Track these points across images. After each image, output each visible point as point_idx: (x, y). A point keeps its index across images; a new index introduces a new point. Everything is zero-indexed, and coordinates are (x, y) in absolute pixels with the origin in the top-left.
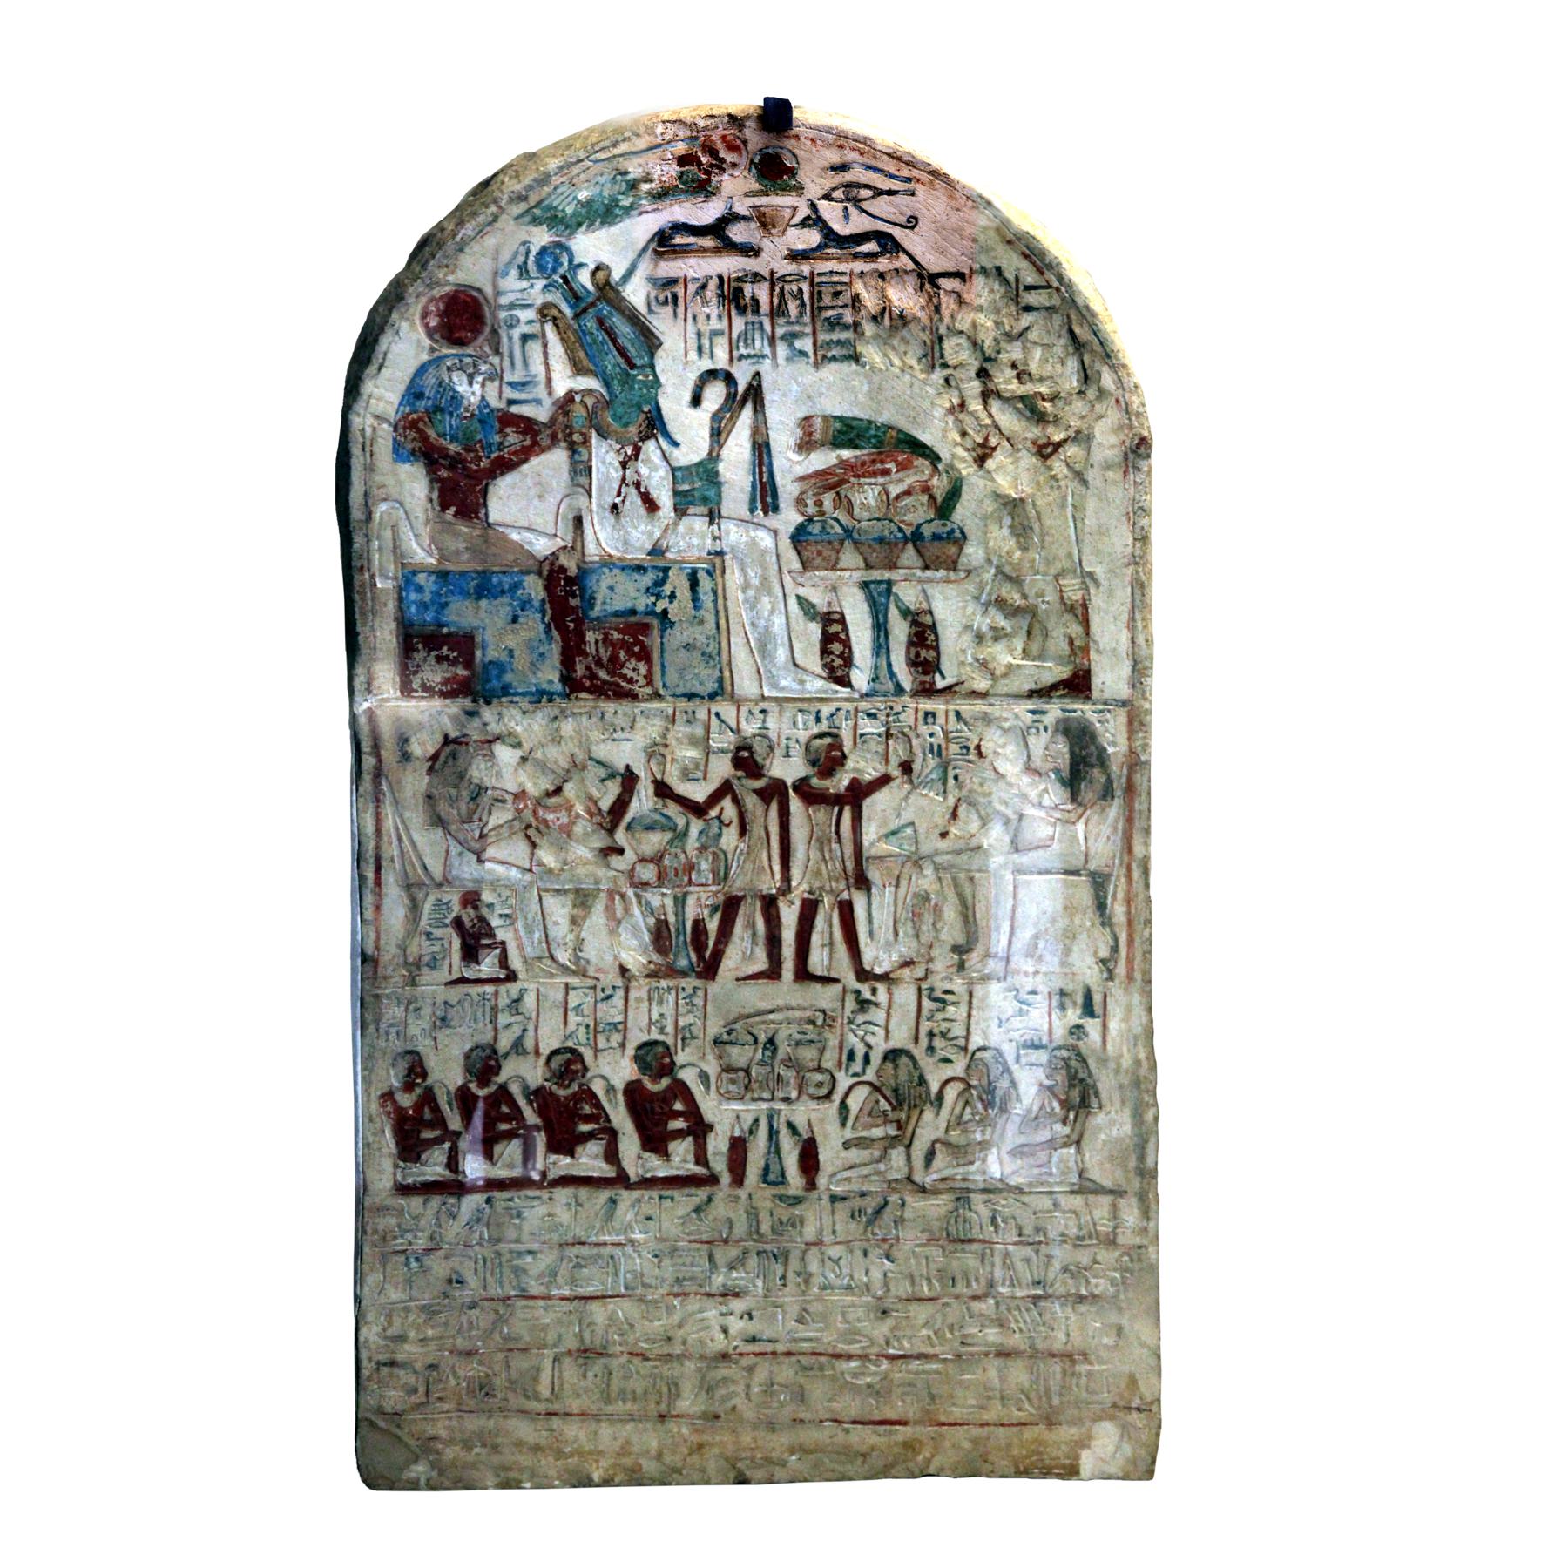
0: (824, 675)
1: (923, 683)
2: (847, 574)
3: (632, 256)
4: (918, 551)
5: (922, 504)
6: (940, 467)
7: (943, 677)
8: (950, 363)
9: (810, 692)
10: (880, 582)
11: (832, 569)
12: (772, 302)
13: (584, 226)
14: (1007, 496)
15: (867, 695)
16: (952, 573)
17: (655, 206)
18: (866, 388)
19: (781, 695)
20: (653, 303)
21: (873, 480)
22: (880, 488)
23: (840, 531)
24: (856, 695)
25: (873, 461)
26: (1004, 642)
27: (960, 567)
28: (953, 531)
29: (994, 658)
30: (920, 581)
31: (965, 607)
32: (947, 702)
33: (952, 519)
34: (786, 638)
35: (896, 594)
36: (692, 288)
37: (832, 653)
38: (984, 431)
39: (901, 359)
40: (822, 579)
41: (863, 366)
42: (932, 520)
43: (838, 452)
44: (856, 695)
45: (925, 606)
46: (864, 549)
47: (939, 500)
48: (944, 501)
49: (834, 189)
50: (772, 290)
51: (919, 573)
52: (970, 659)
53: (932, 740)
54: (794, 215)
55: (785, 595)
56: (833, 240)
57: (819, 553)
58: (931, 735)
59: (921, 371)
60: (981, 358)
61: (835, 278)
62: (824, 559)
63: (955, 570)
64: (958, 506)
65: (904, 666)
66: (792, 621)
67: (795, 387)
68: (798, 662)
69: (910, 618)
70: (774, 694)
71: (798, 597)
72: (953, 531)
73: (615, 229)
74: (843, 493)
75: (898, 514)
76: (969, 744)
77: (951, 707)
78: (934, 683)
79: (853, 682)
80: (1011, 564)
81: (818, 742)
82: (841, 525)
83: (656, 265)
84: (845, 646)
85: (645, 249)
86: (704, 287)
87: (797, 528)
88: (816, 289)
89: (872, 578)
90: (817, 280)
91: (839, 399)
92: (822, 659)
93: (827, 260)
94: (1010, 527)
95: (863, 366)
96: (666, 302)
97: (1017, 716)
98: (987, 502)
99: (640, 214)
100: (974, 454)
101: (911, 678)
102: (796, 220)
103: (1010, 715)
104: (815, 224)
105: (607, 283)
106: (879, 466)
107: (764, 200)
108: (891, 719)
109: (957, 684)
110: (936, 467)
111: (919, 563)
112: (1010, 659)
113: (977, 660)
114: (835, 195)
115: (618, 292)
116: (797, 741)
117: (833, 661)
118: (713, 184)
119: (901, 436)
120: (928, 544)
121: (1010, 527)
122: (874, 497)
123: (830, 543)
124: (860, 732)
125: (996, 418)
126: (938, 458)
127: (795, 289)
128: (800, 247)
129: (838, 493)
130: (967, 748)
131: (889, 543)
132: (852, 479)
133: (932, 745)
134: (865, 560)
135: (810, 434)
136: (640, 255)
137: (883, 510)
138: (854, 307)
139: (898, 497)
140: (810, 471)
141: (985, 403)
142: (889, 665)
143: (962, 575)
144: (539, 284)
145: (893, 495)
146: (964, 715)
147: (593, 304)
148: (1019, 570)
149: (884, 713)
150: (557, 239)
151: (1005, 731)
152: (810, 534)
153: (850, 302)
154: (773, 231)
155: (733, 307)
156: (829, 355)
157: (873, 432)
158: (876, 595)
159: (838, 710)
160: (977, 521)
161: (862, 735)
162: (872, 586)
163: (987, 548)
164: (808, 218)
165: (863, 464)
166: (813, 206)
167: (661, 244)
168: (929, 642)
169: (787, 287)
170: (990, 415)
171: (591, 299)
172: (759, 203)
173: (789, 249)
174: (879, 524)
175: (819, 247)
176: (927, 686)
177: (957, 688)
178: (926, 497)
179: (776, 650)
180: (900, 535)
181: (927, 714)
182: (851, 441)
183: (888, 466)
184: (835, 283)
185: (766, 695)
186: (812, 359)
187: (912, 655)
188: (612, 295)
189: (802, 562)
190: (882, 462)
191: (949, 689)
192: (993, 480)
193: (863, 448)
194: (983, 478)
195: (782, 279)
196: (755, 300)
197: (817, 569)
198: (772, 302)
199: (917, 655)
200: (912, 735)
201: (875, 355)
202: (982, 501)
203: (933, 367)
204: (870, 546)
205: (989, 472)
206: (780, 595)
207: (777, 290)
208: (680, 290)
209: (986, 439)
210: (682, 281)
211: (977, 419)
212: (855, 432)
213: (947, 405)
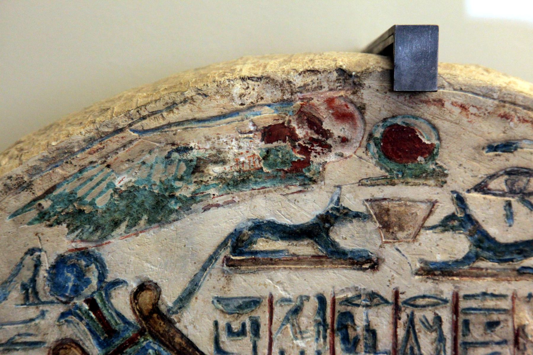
3: (192, 269)
12: (395, 335)
13: (123, 226)
17: (229, 198)
20: (224, 337)
36: (280, 312)
49: (492, 177)
50: (396, 318)
54: (431, 212)
56: (488, 249)
61: (490, 303)
73: (168, 231)
83: (229, 279)
85: (212, 258)
86: (297, 311)
88: (462, 317)
90: (463, 304)
93: (478, 276)
96: (242, 332)
99: (205, 209)
102: (436, 219)
104: (462, 225)
105: (155, 308)
107: (388, 191)
114: (493, 185)
115: (171, 323)
118: (314, 167)
127: (430, 316)
128: (439, 258)
136: (204, 269)
138: (516, 343)
144: (58, 309)
147: (133, 341)
150: (82, 245)
153: (511, 337)
154: (401, 235)
155: (338, 339)
164: (452, 217)
166: (460, 200)
167: (235, 250)
169: (419, 314)
171: (130, 334)
172: (380, 195)
173: (422, 261)
175: (467, 259)
184: (490, 310)
188: (161, 326)
195: (411, 302)
196: (371, 332)
198: (395, 335)
207: (404, 317)
208: (262, 314)
210: (266, 302)
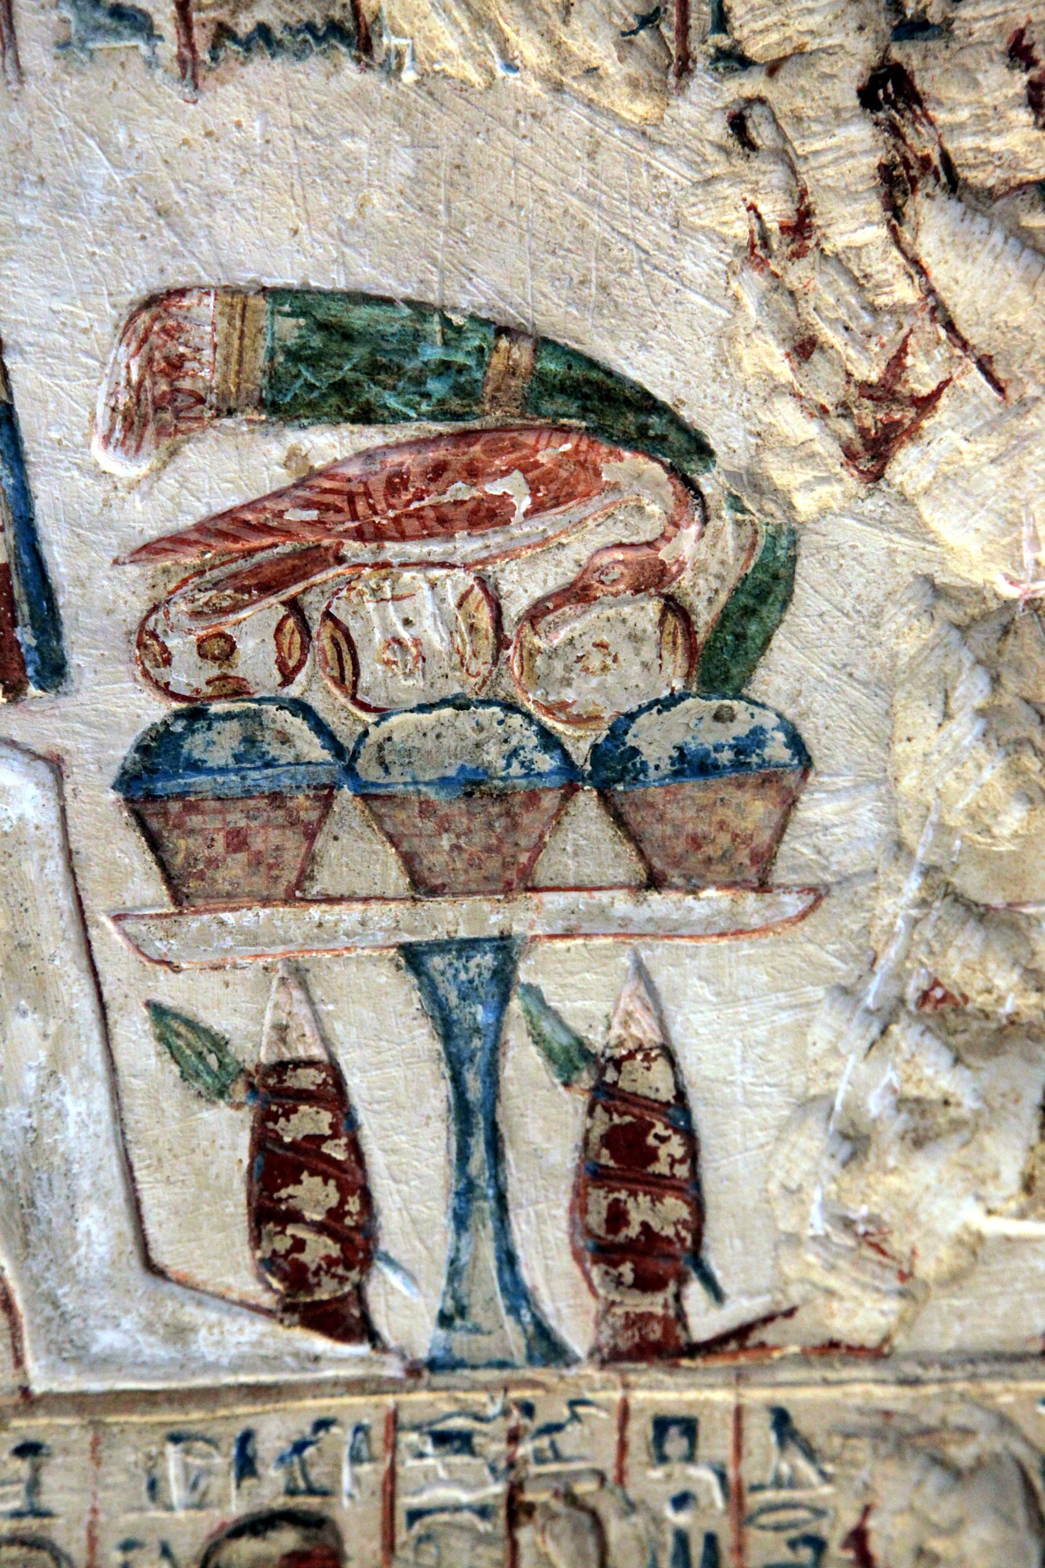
0: (267, 1300)
1: (638, 1321)
2: (349, 915)
4: (620, 821)
5: (635, 638)
6: (709, 483)
7: (717, 1295)
8: (753, 50)
9: (212, 1367)
10: (468, 946)
11: (289, 899)
14: (977, 593)
15: (433, 1365)
16: (750, 900)
18: (403, 163)
19: (95, 1385)
21: (436, 549)
22: (466, 579)
23: (315, 750)
24: (393, 1368)
25: (438, 470)
26: (950, 1150)
27: (780, 874)
28: (757, 737)
29: (911, 1215)
30: (625, 933)
31: (801, 1030)
32: (741, 1378)
33: (756, 690)
34: (114, 1168)
35: (532, 991)
37: (295, 1217)
38: (890, 334)
39: (547, 35)
40: (251, 938)
41: (392, 70)
42: (673, 700)
43: (293, 437)
44: (393, 1368)
45: (645, 1031)
46: (402, 818)
47: (704, 618)
48: (725, 616)
51: (622, 904)
52: (818, 1224)
53: (682, 1519)
55: (103, 1007)
57: (237, 841)
58: (681, 1501)
59: (634, 83)
60: (884, 23)
62: (257, 861)
63: (763, 887)
64: (779, 640)
65: (565, 1262)
66: (137, 1113)
67: (102, 170)
68: (161, 1255)
69: (586, 1079)
70: (71, 1382)
71: (158, 1012)
72: (757, 737)
74: (314, 606)
75: (536, 679)
76: (823, 1528)
77: (757, 1396)
78: (681, 1317)
79: (381, 1322)
80: (985, 858)
81: (247, 1547)
82: (320, 728)
84: (345, 1191)
87: (142, 749)
89: (439, 934)
91: (290, 212)
92: (256, 1240)
94: (981, 713)
95: (392, 70)
97: (1005, 1422)
98: (896, 618)
100: (847, 429)
101: (593, 1305)
103: (975, 1418)
106: (460, 490)
108: (525, 1449)
109: (768, 1319)
110: (690, 484)
111: (629, 866)
112: (973, 1216)
113: (848, 1224)
116: (166, 1552)
117: (299, 1245)
119: (552, 366)
120: (656, 794)
121: (981, 713)
122: (440, 615)
123: (276, 798)
124: (406, 1501)
125: (939, 275)
126: (703, 451)
129: (294, 606)
130: (818, 1544)
131: (502, 796)
132: (352, 548)
133: (682, 1539)
134: (409, 861)
135: (175, 365)
137: (480, 666)
139: (535, 614)
140: (187, 521)
141: (895, 212)
142: (508, 1259)
143: (792, 904)
145: (514, 608)
146: (802, 1423)
148: (1018, 880)
149: (500, 1427)
151: (957, 1474)
152: (195, 766)
156: (245, 24)
157: (433, 352)
158: (454, 999)
159: (323, 1424)
160: (855, 694)
161: (415, 1515)
162: (437, 962)
163: (891, 799)
165: (396, 483)
168: (661, 1167)
170: (917, 267)
174: (465, 721)
176: (655, 1332)
177: (768, 1335)
178: (653, 607)
179: (72, 1219)
180: (546, 762)
181: (662, 1425)
182: (341, 387)
183: (495, 488)
185: (38, 1388)
186: (169, 47)
187: (596, 1219)
189: (168, 879)
190: (473, 473)
191: (741, 1333)
192: (921, 531)
193: (398, 417)
194: (879, 522)
197: (231, 900)
199: (617, 1217)
200: (607, 1507)
201: (438, 24)
202: (876, 618)
203: (684, 67)
204: (426, 809)
205: (904, 500)
206: (86, 1007)
209: (897, 364)
211: (859, 283)
212: (359, 353)
213: (741, 229)
